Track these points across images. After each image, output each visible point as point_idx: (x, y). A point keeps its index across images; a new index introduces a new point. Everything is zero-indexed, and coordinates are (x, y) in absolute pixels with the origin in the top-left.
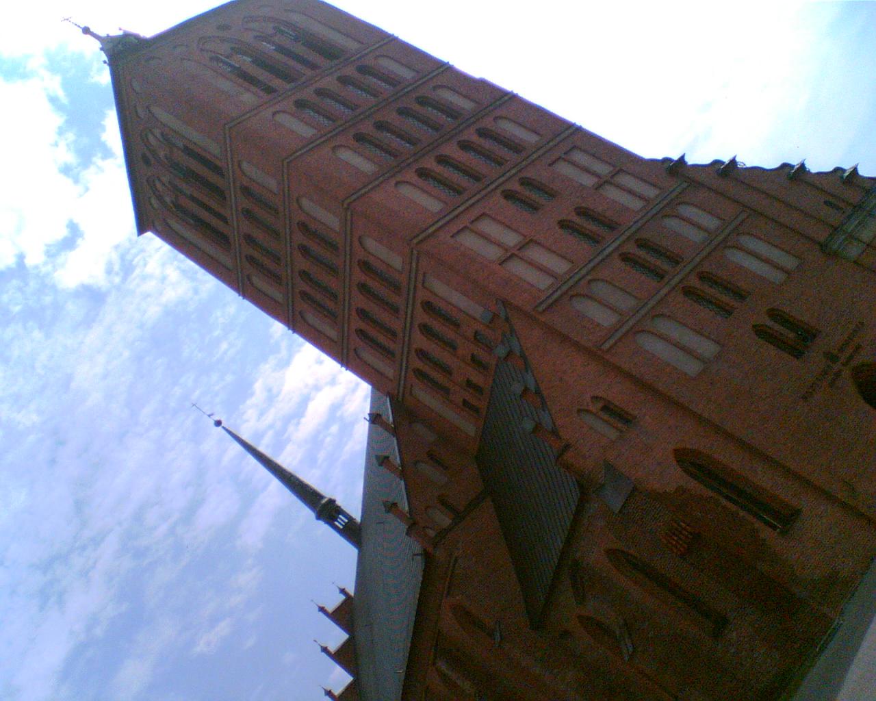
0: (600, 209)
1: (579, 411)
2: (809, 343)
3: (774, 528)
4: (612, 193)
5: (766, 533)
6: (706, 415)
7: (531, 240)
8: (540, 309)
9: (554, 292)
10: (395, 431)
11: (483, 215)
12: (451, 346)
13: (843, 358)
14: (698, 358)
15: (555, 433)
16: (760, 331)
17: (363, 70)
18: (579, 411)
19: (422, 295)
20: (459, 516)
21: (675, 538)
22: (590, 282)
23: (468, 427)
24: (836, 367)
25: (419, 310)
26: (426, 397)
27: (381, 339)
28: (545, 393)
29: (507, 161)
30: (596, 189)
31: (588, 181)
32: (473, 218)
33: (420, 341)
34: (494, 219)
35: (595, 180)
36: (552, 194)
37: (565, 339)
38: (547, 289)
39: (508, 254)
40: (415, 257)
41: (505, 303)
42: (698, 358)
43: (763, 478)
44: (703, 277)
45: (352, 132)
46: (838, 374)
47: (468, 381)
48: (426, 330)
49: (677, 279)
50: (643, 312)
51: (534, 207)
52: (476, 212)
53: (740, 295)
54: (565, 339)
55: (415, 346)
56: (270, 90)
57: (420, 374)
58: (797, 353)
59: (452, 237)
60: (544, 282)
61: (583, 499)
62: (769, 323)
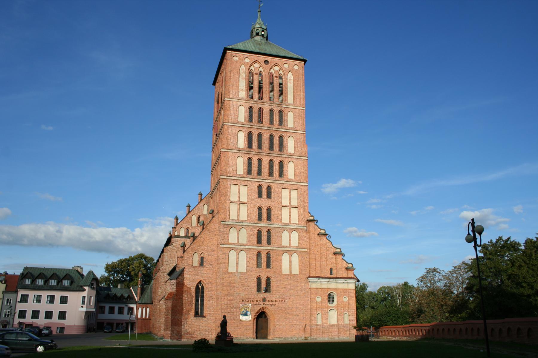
5: (192, 313)
8: (222, 223)
13: (267, 303)
14: (237, 269)
17: (281, 112)
24: (262, 303)
28: (195, 241)
42: (237, 269)
45: (250, 130)
46: (258, 304)
50: (243, 247)
52: (245, 183)
56: (251, 97)
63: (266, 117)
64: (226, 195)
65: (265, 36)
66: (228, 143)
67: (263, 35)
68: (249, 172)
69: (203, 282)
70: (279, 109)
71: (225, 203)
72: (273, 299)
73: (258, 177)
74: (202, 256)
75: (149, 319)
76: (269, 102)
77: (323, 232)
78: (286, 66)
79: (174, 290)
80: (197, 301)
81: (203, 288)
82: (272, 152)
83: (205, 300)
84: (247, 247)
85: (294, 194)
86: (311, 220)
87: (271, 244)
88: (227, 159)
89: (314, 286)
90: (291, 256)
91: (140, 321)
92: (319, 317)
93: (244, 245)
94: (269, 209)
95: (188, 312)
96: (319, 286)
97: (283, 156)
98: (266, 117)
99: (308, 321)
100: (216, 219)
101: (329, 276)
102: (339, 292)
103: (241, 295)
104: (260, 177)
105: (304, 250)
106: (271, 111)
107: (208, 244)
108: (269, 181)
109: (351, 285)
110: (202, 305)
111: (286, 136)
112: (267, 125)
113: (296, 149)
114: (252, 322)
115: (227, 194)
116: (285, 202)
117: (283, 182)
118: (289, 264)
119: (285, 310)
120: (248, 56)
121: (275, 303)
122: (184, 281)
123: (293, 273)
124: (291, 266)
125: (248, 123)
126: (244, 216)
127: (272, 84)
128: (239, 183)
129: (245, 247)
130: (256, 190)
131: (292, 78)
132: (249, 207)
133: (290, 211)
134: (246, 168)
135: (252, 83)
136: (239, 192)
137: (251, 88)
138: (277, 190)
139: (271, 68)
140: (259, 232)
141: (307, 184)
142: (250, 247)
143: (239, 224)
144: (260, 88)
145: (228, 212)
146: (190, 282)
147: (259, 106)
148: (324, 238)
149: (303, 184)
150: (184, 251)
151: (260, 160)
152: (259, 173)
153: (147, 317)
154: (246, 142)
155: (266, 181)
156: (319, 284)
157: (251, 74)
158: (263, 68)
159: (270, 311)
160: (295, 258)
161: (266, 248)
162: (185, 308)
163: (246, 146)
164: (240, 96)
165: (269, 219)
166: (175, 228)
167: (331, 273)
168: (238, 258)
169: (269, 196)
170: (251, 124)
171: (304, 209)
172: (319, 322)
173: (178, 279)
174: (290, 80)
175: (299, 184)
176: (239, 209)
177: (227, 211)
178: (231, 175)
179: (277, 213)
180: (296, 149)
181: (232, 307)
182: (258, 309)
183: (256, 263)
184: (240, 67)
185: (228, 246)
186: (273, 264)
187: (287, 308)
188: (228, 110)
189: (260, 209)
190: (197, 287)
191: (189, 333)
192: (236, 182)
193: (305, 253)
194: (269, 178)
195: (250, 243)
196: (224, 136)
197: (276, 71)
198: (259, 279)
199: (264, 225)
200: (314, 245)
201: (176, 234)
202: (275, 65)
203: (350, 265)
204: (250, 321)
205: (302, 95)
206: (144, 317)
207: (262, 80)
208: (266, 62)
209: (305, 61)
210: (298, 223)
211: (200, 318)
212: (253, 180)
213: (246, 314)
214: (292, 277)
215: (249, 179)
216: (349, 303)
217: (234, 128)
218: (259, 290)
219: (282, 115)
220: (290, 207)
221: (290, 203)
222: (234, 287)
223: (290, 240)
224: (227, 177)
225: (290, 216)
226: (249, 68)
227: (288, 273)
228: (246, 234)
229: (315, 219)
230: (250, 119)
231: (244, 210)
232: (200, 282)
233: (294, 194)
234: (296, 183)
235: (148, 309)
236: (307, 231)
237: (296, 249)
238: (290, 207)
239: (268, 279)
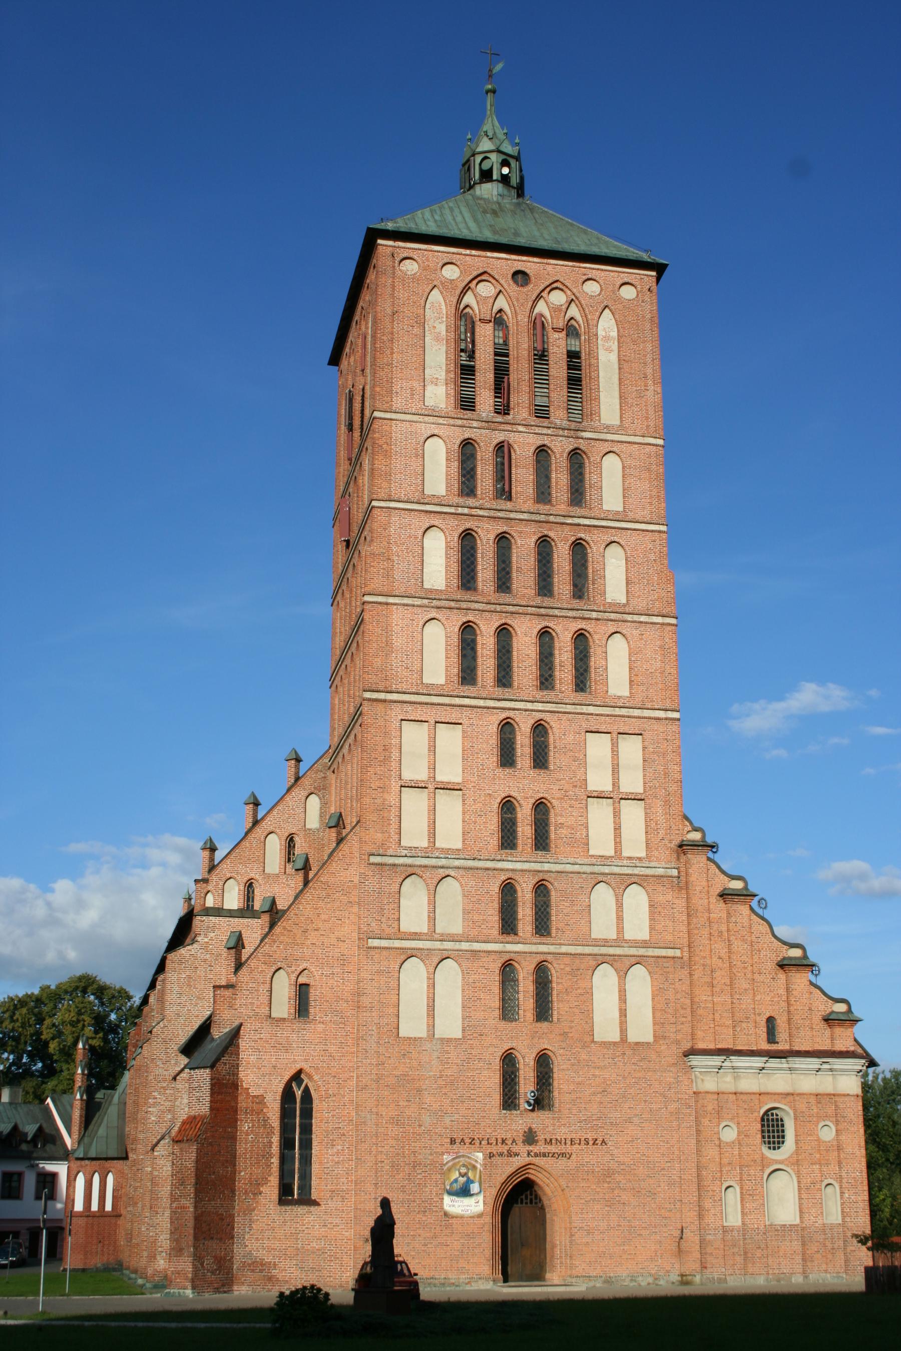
8: (373, 859)
14: (431, 1026)
17: (576, 456)
24: (522, 1149)
28: (277, 929)
38: (406, 848)
42: (431, 1026)
45: (468, 525)
46: (510, 1154)
52: (454, 715)
56: (467, 404)
63: (523, 477)
64: (387, 759)
65: (514, 181)
66: (388, 574)
67: (505, 179)
68: (468, 674)
69: (310, 1077)
70: (569, 445)
71: (384, 789)
72: (562, 1133)
73: (499, 692)
74: (302, 980)
75: (116, 1214)
76: (533, 420)
77: (737, 885)
78: (592, 288)
79: (204, 1108)
80: (287, 1144)
81: (307, 1096)
82: (547, 601)
83: (315, 1143)
84: (465, 946)
85: (631, 750)
86: (694, 845)
87: (549, 934)
88: (387, 629)
89: (709, 1084)
90: (623, 975)
91: (82, 1221)
92: (733, 1198)
93: (453, 938)
94: (541, 808)
95: (256, 1186)
96: (727, 1083)
97: (587, 614)
98: (523, 477)
99: (690, 1216)
100: (352, 844)
101: (765, 1046)
102: (802, 1106)
103: (447, 1120)
104: (507, 693)
105: (670, 953)
106: (542, 452)
107: (325, 937)
108: (540, 706)
109: (847, 1081)
110: (306, 1160)
111: (595, 542)
112: (530, 505)
113: (635, 589)
114: (488, 1219)
115: (389, 755)
116: (599, 780)
117: (591, 709)
118: (619, 1006)
119: (608, 1174)
120: (455, 258)
121: (569, 1148)
122: (241, 1075)
123: (633, 1036)
124: (623, 1013)
125: (461, 500)
126: (450, 835)
127: (541, 356)
128: (431, 715)
129: (457, 946)
130: (494, 741)
131: (614, 334)
133: (617, 814)
134: (455, 659)
135: (472, 356)
136: (432, 748)
137: (467, 371)
138: (570, 738)
139: (539, 297)
140: (508, 890)
141: (676, 715)
142: (477, 946)
143: (433, 862)
144: (501, 372)
145: (394, 820)
146: (260, 1079)
147: (500, 437)
148: (744, 910)
149: (661, 714)
150: (239, 966)
151: (504, 633)
152: (504, 677)
153: (108, 1207)
154: (455, 567)
155: (529, 706)
156: (729, 1078)
157: (464, 321)
158: (509, 299)
159: (551, 1179)
160: (640, 982)
161: (534, 948)
162: (244, 1173)
163: (455, 582)
164: (429, 402)
165: (541, 841)
166: (205, 881)
167: (771, 1036)
168: (432, 986)
169: (540, 760)
170: (471, 502)
171: (667, 803)
172: (734, 1219)
173: (219, 1066)
174: (607, 338)
175: (647, 713)
176: (433, 810)
177: (389, 818)
178: (404, 687)
179: (571, 821)
180: (635, 589)
182: (510, 1170)
183: (496, 1003)
184: (426, 297)
185: (397, 944)
186: (559, 1007)
187: (613, 1165)
188: (387, 454)
189: (508, 806)
190: (287, 1095)
191: (258, 1266)
192: (418, 714)
193: (673, 965)
194: (539, 695)
195: (473, 933)
196: (375, 548)
197: (555, 310)
198: (509, 1061)
199: (523, 865)
200: (705, 932)
201: (210, 902)
202: (552, 287)
203: (841, 1008)
204: (480, 1216)
205: (650, 393)
206: (95, 1207)
207: (506, 343)
208: (520, 277)
209: (660, 269)
210: (648, 857)
211: (301, 1210)
212: (481, 703)
213: (464, 1192)
214: (629, 1052)
215: (467, 701)
216: (839, 1148)
217: (407, 518)
218: (509, 1101)
219: (581, 466)
220: (616, 798)
221: (616, 784)
222: (419, 1090)
223: (620, 919)
224: (390, 697)
225: (617, 829)
226: (459, 301)
227: (616, 1037)
228: (460, 898)
229: (709, 840)
230: (467, 483)
231: (451, 810)
232: (297, 1077)
233: (631, 750)
234: (637, 712)
235: (110, 1179)
236: (681, 884)
237: (642, 951)
238: (616, 798)
239: (543, 1062)
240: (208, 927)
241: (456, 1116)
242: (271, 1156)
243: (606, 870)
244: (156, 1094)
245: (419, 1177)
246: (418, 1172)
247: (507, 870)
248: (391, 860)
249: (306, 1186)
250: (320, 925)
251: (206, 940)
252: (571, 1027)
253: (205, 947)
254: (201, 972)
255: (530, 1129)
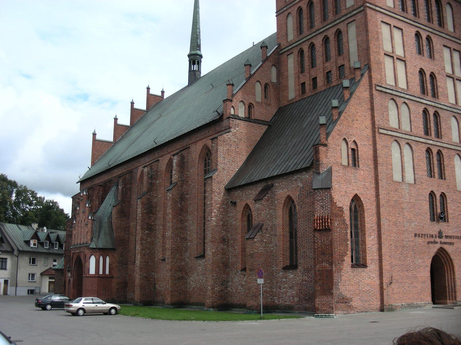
0: (439, 84)
1: (345, 139)
2: (440, 221)
3: (352, 261)
4: (449, 83)
5: (348, 259)
6: (381, 197)
7: (405, 61)
9: (389, 89)
10: (266, 60)
11: (401, 29)
12: (327, 58)
13: (444, 240)
15: (328, 135)
16: (432, 194)
18: (345, 139)
19: (342, 27)
20: (248, 119)
21: (321, 221)
22: (405, 102)
23: (292, 93)
25: (334, 30)
26: (291, 62)
27: (305, 22)
28: (342, 118)
29: (433, 23)
30: (447, 76)
31: (449, 70)
32: (397, 26)
33: (318, 42)
34: (403, 36)
35: (451, 72)
36: (431, 56)
37: (372, 109)
39: (392, 55)
40: (359, 10)
41: (369, 69)
43: (371, 241)
44: (439, 153)
47: (316, 78)
48: (326, 40)
49: (431, 142)
50: (407, 137)
51: (420, 52)
53: (442, 176)
54: (372, 109)
55: (313, 40)
57: (301, 52)
58: (433, 219)
59: (382, 21)
60: (390, 81)
61: (306, 169)
62: (438, 197)
64: (378, 39)
71: (378, 53)
132: (408, 67)
142: (417, 139)
178: (381, 5)
181: (403, 247)
186: (447, 173)
192: (387, 19)
240: (236, 125)
241: (416, 223)
242: (348, 240)
243: (455, 110)
244: (215, 210)
245: (405, 253)
246: (405, 250)
247: (425, 104)
248: (384, 90)
249: (357, 259)
250: (358, 118)
251: (235, 131)
252: (450, 183)
253: (235, 135)
254: (233, 148)
255: (440, 230)
